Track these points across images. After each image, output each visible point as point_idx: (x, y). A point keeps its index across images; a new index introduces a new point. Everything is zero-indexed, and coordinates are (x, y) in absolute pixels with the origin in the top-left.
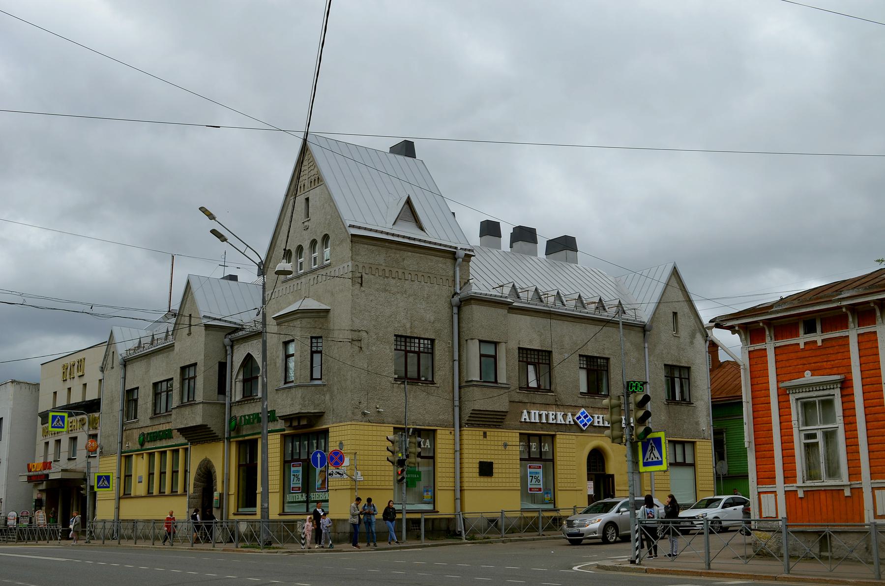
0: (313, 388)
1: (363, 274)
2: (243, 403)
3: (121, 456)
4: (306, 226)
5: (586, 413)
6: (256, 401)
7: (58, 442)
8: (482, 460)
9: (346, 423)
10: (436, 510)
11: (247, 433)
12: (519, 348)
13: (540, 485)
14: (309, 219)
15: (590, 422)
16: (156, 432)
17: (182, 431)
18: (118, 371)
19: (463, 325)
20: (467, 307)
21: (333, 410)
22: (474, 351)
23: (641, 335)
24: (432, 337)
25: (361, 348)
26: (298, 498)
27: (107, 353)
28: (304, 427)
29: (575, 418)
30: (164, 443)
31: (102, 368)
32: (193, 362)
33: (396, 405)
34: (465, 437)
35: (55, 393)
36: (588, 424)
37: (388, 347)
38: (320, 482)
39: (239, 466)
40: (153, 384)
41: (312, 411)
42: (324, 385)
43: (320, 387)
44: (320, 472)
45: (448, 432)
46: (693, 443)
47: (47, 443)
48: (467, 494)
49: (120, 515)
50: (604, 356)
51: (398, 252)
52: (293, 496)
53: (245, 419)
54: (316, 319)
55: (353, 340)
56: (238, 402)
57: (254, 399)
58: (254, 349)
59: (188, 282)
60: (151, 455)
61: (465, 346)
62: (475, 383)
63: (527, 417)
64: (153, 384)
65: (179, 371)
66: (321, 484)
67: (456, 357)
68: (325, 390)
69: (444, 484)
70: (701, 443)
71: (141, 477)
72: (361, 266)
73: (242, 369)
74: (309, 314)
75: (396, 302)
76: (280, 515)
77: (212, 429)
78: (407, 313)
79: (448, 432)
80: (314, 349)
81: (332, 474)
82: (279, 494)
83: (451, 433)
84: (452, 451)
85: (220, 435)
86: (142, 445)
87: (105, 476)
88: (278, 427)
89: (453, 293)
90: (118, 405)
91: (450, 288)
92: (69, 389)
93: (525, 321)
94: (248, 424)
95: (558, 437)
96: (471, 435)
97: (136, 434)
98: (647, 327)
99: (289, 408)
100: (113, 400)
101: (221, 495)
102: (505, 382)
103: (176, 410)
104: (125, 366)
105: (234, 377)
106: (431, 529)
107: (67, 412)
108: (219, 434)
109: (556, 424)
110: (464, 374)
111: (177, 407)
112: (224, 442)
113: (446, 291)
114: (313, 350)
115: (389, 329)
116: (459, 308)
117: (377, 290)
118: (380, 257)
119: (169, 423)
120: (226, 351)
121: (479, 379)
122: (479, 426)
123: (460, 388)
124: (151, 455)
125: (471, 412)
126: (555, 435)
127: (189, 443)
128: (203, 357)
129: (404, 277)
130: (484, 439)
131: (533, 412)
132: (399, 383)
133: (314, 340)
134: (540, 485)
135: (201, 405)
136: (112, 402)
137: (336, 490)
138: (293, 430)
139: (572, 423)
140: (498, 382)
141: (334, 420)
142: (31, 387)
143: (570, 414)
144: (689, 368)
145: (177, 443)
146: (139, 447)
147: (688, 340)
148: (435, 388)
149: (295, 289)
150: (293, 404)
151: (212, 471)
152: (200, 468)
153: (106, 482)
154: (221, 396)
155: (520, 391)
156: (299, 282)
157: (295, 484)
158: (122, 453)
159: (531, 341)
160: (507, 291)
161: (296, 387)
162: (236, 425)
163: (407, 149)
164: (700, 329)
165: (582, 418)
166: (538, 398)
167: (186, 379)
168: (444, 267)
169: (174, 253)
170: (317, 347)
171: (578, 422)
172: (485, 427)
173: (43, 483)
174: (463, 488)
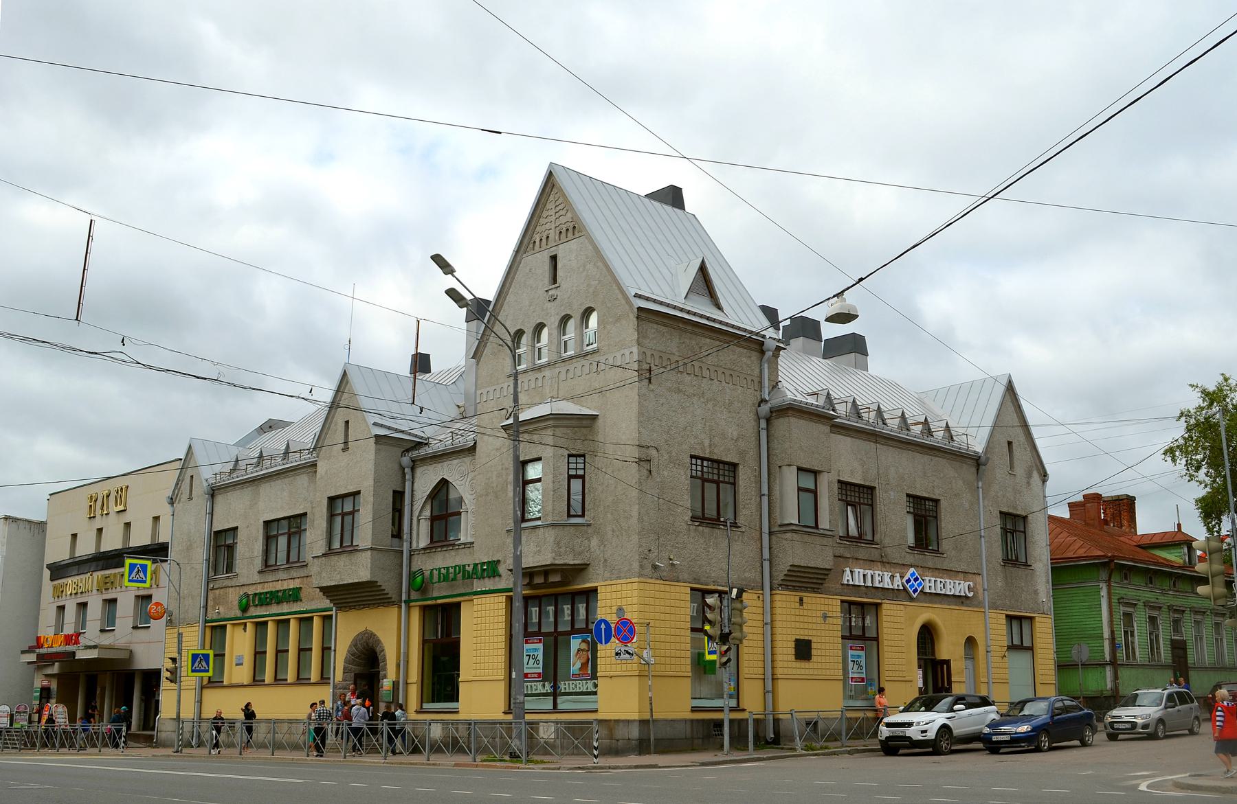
0: (572, 528)
1: (652, 365)
2: (440, 549)
3: (205, 626)
4: (552, 296)
5: (917, 574)
6: (457, 547)
7: (83, 606)
8: (798, 637)
9: (629, 580)
10: (741, 707)
11: (440, 594)
12: (839, 482)
13: (863, 673)
14: (556, 285)
15: (921, 587)
16: (272, 592)
17: (325, 590)
18: (201, 502)
19: (775, 445)
20: (781, 420)
21: (605, 561)
22: (790, 481)
23: (974, 470)
24: (735, 461)
25: (650, 471)
26: (536, 690)
27: (181, 478)
28: (555, 584)
29: (904, 581)
30: (285, 608)
31: (172, 498)
32: (351, 489)
33: (693, 556)
34: (777, 604)
35: (74, 536)
36: (919, 590)
37: (682, 473)
38: (578, 665)
39: (424, 642)
40: (264, 522)
41: (571, 562)
42: (589, 525)
43: (582, 528)
44: (578, 651)
45: (755, 597)
46: (1031, 619)
47: (61, 609)
48: (781, 685)
49: (202, 712)
50: (934, 497)
51: (694, 337)
53: (439, 574)
54: (576, 429)
55: (640, 460)
56: (424, 549)
57: (454, 545)
58: (450, 471)
59: (345, 374)
60: (261, 626)
61: (778, 475)
62: (794, 528)
63: (850, 578)
64: (264, 522)
65: (325, 502)
67: (765, 490)
68: (589, 531)
69: (751, 671)
70: (1042, 620)
71: (241, 657)
72: (649, 354)
73: (429, 502)
74: (565, 422)
75: (691, 409)
76: (505, 713)
77: (383, 588)
78: (705, 425)
79: (755, 597)
80: (572, 472)
81: (620, 653)
82: (503, 683)
83: (759, 597)
84: (760, 624)
85: (394, 596)
86: (245, 610)
87: (202, 654)
88: (502, 585)
89: (759, 399)
90: (201, 553)
91: (755, 392)
92: (100, 530)
93: (844, 443)
94: (444, 581)
95: (884, 606)
96: (785, 601)
97: (233, 596)
98: (983, 459)
99: (533, 556)
100: (191, 545)
101: (396, 685)
102: (828, 528)
103: (320, 559)
104: (213, 496)
105: (416, 513)
106: (737, 734)
107: (150, 559)
108: (393, 594)
109: (883, 589)
110: (777, 513)
111: (323, 554)
112: (400, 607)
113: (751, 397)
114: (570, 473)
115: (684, 447)
116: (768, 420)
117: (669, 390)
118: (673, 344)
119: (294, 579)
120: (404, 475)
121: (797, 523)
122: (794, 588)
123: (771, 533)
124: (261, 626)
125: (788, 568)
126: (881, 604)
127: (334, 608)
128: (371, 482)
129: (702, 374)
130: (801, 607)
131: (857, 570)
132: (697, 524)
133: (572, 460)
134: (863, 673)
135: (369, 553)
136: (189, 548)
137: (611, 677)
139: (901, 588)
140: (820, 527)
141: (607, 575)
142: (33, 526)
143: (898, 575)
144: (1025, 518)
145: (309, 608)
146: (239, 614)
147: (1024, 480)
148: (739, 533)
149: (533, 386)
150: (540, 551)
151: (378, 650)
152: (355, 643)
153: (204, 663)
154: (396, 540)
155: (841, 542)
156: (540, 375)
157: (531, 668)
158: (206, 621)
159: (852, 472)
160: (821, 401)
161: (544, 526)
162: (423, 581)
163: (673, 197)
164: (1036, 466)
165: (912, 581)
166: (862, 553)
167: (338, 514)
168: (749, 362)
169: (419, 317)
170: (576, 469)
171: (908, 586)
172: (802, 591)
173: (54, 664)
174: (775, 677)
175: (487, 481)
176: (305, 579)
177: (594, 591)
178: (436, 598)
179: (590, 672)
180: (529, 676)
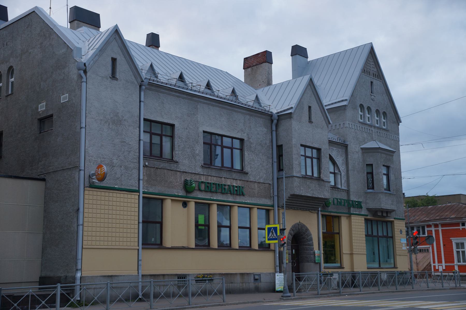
30: (230, 198)
88: (363, 213)
103: (299, 179)
119: (236, 179)
138: (373, 217)
152: (292, 229)
177: (392, 222)
178: (330, 212)
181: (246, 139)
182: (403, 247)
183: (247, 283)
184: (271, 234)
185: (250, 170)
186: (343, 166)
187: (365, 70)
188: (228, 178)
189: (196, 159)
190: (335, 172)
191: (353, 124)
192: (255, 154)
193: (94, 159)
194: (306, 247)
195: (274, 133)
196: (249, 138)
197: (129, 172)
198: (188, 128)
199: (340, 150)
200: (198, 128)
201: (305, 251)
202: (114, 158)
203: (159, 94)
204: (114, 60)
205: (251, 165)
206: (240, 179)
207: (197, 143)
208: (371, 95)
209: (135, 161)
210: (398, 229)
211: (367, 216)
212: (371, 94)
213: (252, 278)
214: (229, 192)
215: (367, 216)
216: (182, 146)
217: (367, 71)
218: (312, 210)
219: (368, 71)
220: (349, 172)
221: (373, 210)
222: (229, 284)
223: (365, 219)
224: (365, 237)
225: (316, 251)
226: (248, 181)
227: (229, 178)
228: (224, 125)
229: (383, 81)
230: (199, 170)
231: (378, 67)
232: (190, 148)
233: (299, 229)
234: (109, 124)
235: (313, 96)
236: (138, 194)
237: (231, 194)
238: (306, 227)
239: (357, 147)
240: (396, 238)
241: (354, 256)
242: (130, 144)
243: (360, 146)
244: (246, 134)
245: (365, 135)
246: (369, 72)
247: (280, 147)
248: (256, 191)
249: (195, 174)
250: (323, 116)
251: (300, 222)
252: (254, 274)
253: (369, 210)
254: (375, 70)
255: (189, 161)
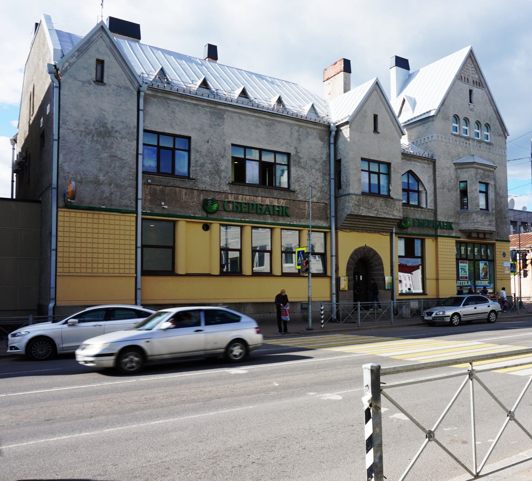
26: (464, 284)
38: (483, 274)
52: (460, 283)
66: (484, 276)
88: (454, 235)
119: (278, 199)
157: (462, 274)
175: (443, 182)
176: (291, 201)
177: (493, 245)
179: (488, 277)
180: (462, 278)
181: (293, 153)
182: (506, 271)
183: (291, 313)
184: (300, 258)
185: (299, 188)
186: (430, 184)
187: (461, 77)
188: (266, 197)
189: (221, 176)
190: (420, 190)
191: (444, 137)
192: (306, 170)
193: (71, 176)
194: (375, 272)
195: (332, 146)
196: (297, 152)
197: (122, 191)
198: (210, 141)
199: (426, 166)
200: (224, 141)
201: (374, 277)
202: (100, 174)
203: (168, 101)
204: (100, 63)
205: (300, 183)
206: (283, 198)
207: (223, 157)
208: (469, 105)
209: (131, 178)
210: (501, 252)
211: (459, 238)
212: (470, 104)
213: (299, 307)
214: (268, 213)
215: (459, 238)
216: (201, 162)
217: (465, 78)
218: (383, 232)
219: (466, 78)
220: (437, 189)
221: (467, 231)
222: (266, 314)
223: (456, 242)
224: (455, 261)
225: (386, 277)
226: (294, 200)
227: (268, 197)
228: (262, 138)
229: (487, 89)
230: (226, 188)
231: (480, 74)
232: (213, 164)
233: (364, 253)
234: (93, 136)
235: (381, 102)
236: (135, 215)
237: (270, 214)
238: (375, 251)
239: (448, 162)
240: (497, 262)
241: (440, 281)
242: (124, 159)
243: (452, 161)
244: (293, 148)
245: (460, 149)
246: (468, 79)
247: (338, 162)
248: (306, 212)
249: (219, 192)
250: (395, 126)
251: (365, 246)
252: (302, 303)
253: (462, 231)
254: (477, 76)
255: (211, 178)
